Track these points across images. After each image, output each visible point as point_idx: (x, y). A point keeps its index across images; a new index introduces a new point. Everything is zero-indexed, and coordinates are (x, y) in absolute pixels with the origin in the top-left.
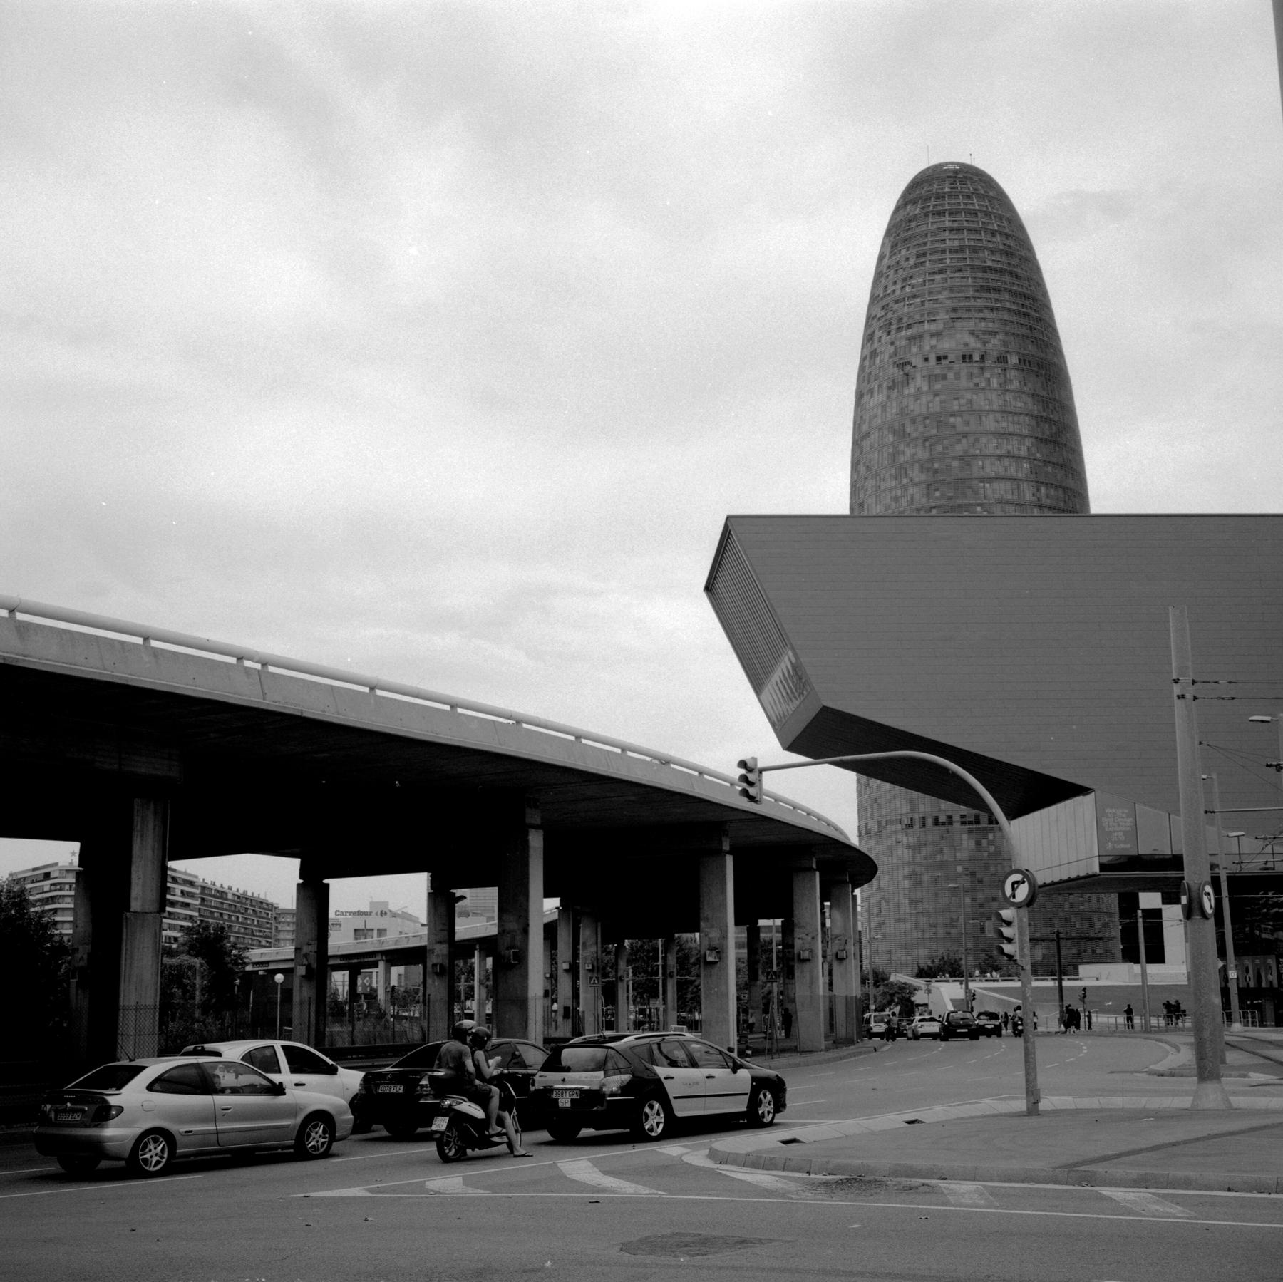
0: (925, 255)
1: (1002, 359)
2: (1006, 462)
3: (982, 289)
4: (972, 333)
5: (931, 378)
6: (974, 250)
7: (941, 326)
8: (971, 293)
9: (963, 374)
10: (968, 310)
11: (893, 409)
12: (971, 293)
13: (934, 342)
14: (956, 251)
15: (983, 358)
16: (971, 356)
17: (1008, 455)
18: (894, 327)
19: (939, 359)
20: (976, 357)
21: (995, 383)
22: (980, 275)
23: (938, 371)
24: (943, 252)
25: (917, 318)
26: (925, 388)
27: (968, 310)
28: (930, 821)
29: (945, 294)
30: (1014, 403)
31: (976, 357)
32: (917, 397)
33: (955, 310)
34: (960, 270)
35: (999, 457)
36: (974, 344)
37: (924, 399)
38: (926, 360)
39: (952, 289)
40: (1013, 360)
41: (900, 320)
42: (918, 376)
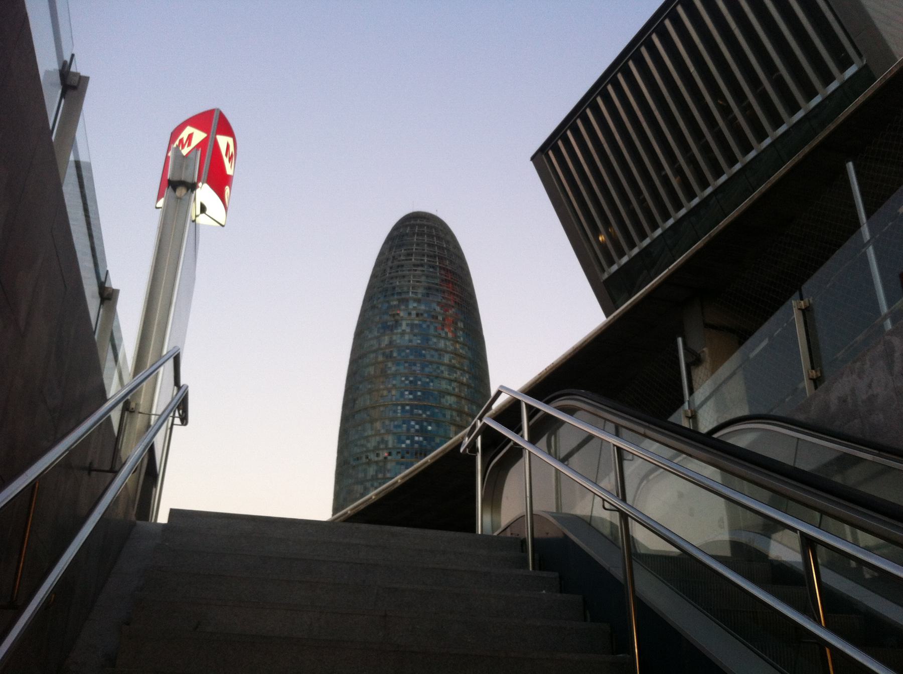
0: (412, 255)
1: (455, 323)
2: (454, 384)
4: (439, 304)
5: (412, 326)
7: (420, 296)
8: (437, 281)
9: (432, 328)
10: (437, 290)
11: (386, 340)
12: (437, 281)
13: (415, 305)
14: (431, 256)
15: (444, 319)
16: (437, 318)
17: (455, 380)
18: (389, 293)
19: (417, 315)
20: (440, 318)
21: (450, 335)
22: (443, 272)
23: (416, 322)
24: (424, 255)
25: (405, 289)
26: (408, 330)
27: (437, 290)
29: (423, 279)
30: (461, 351)
31: (440, 318)
32: (403, 333)
34: (433, 267)
35: (451, 381)
36: (438, 309)
37: (407, 337)
38: (410, 314)
39: (427, 277)
41: (394, 288)
42: (404, 323)
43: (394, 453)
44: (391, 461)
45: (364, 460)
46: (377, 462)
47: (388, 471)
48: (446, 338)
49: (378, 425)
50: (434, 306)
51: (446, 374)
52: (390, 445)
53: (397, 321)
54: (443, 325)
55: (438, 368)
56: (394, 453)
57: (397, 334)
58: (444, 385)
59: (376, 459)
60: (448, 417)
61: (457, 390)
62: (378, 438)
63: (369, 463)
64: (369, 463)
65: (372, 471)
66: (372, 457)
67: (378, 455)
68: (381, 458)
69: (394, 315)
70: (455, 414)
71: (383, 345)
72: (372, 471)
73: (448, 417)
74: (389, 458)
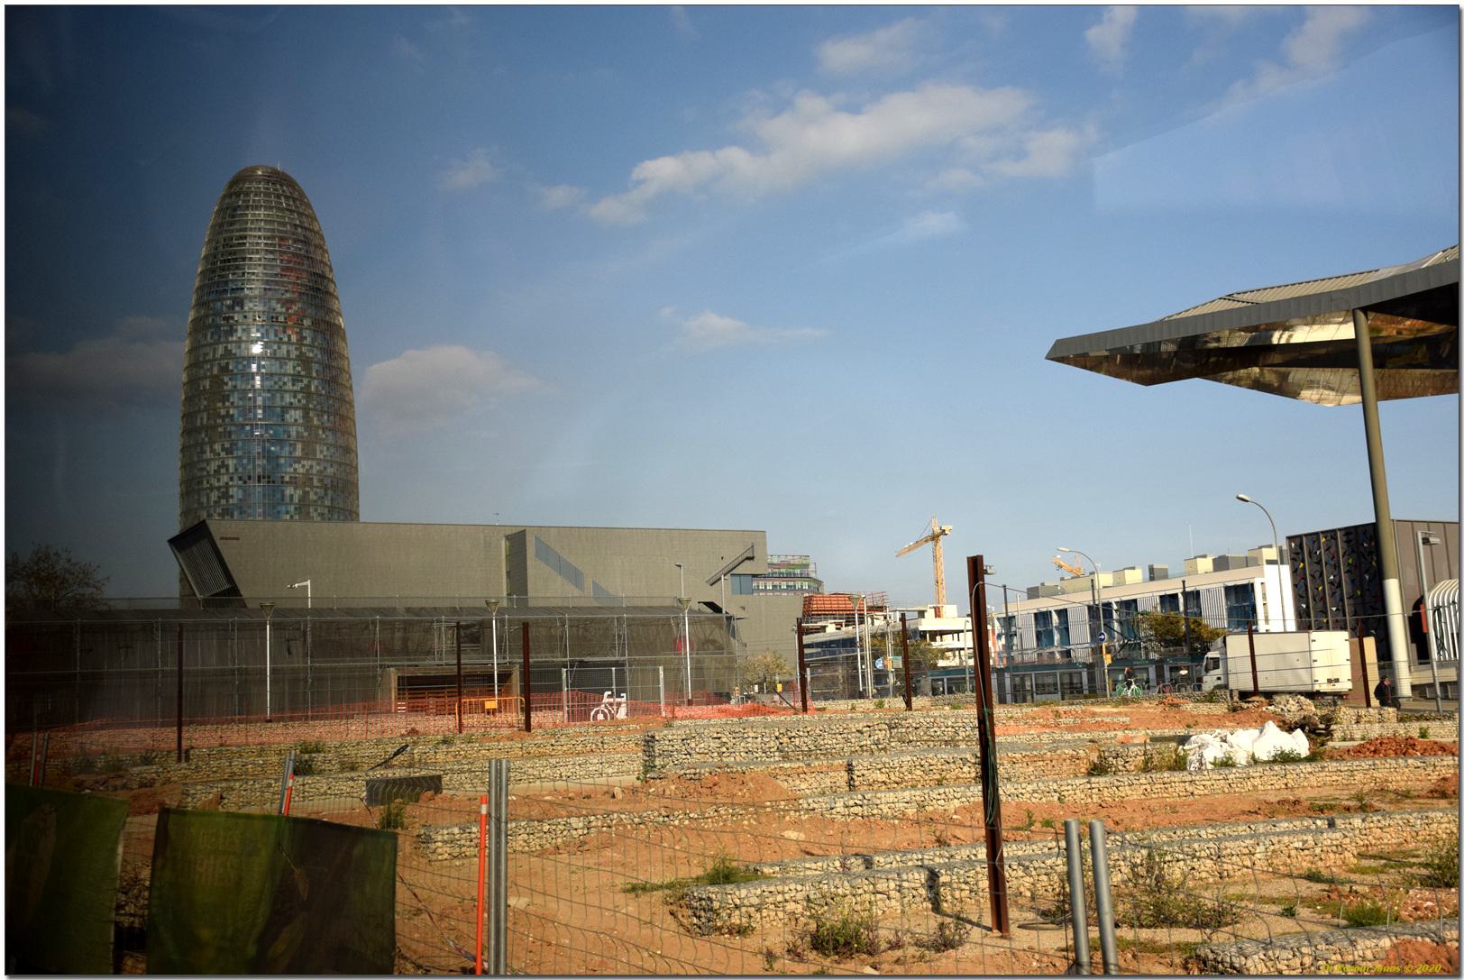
1: (299, 323)
3: (287, 269)
4: (278, 301)
6: (282, 239)
11: (220, 350)
20: (281, 319)
21: (294, 338)
31: (281, 319)
33: (267, 282)
36: (279, 308)
40: (307, 322)
41: (226, 283)
45: (205, 485)
46: (219, 488)
48: (289, 342)
49: (217, 447)
50: (273, 303)
51: (289, 386)
58: (288, 399)
60: (294, 434)
63: (212, 488)
64: (212, 488)
65: (214, 496)
69: (227, 319)
70: (301, 429)
73: (294, 434)
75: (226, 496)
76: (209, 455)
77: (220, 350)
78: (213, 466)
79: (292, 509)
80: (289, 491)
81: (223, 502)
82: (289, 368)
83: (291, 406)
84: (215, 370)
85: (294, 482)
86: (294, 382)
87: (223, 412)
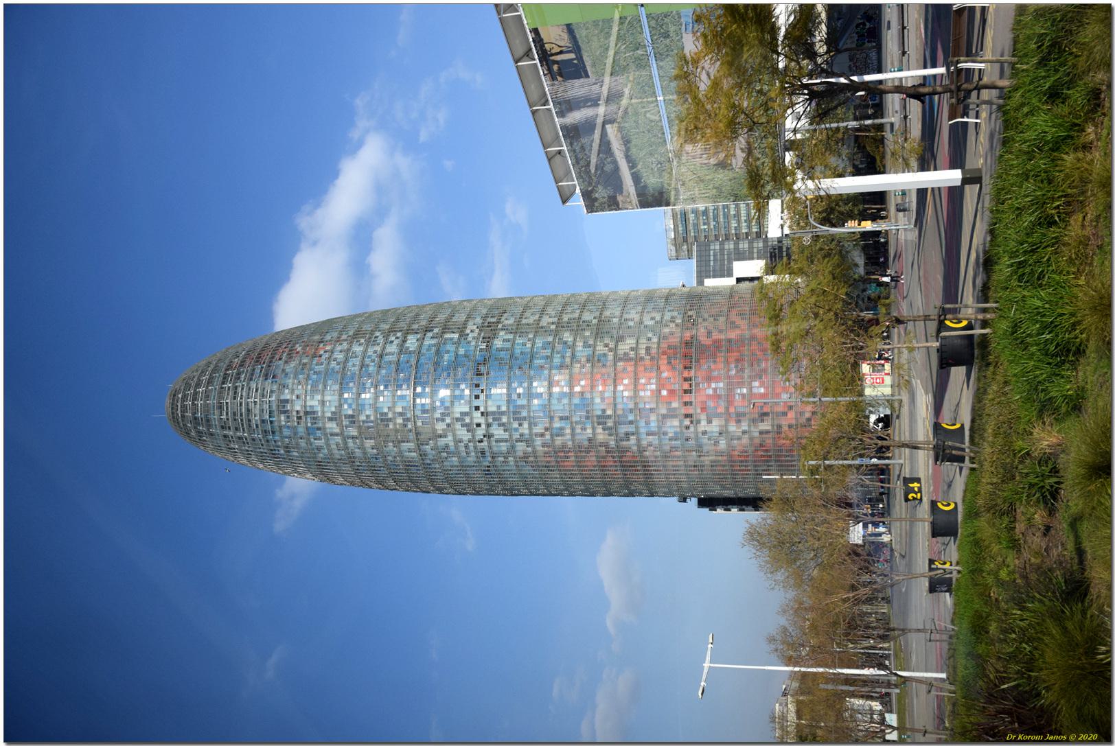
11: (332, 426)
25: (266, 407)
28: (687, 398)
41: (263, 421)
43: (476, 403)
44: (486, 407)
46: (488, 425)
47: (499, 407)
48: (332, 352)
49: (440, 427)
51: (378, 348)
52: (466, 409)
53: (307, 413)
54: (314, 356)
55: (370, 357)
56: (476, 403)
57: (323, 412)
58: (392, 348)
59: (483, 426)
61: (399, 334)
62: (458, 426)
64: (489, 436)
65: (498, 432)
66: (480, 432)
67: (478, 425)
68: (482, 420)
69: (299, 418)
70: (429, 334)
71: (337, 430)
72: (498, 432)
74: (482, 409)
75: (497, 415)
76: (449, 440)
77: (332, 426)
78: (463, 433)
79: (519, 340)
80: (498, 343)
81: (504, 420)
82: (358, 349)
83: (402, 345)
84: (353, 432)
85: (488, 340)
86: (375, 343)
87: (400, 421)
